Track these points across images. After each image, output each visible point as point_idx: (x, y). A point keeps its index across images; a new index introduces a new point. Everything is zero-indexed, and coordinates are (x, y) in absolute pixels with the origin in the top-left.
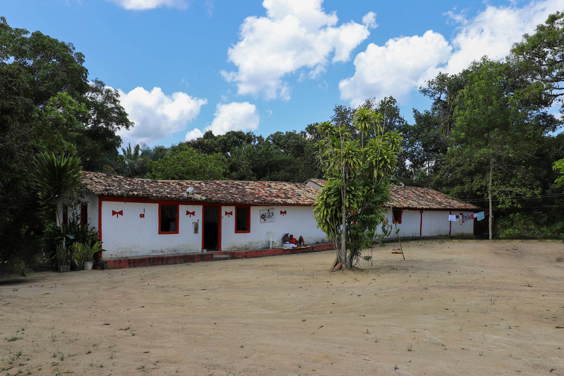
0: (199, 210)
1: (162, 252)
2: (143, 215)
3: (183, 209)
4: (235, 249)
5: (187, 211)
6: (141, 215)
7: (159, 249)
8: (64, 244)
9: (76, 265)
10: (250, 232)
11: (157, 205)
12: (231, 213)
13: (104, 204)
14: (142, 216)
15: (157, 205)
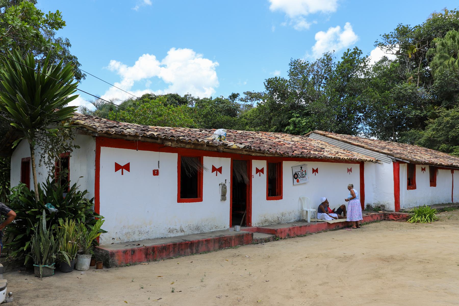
0: (226, 164)
1: (182, 231)
2: (158, 171)
3: (208, 162)
4: (267, 224)
5: (213, 167)
6: (154, 171)
7: (178, 228)
8: (44, 222)
9: (65, 263)
10: (281, 198)
11: (176, 155)
12: (262, 171)
13: (104, 150)
14: (156, 173)
15: (176, 155)
